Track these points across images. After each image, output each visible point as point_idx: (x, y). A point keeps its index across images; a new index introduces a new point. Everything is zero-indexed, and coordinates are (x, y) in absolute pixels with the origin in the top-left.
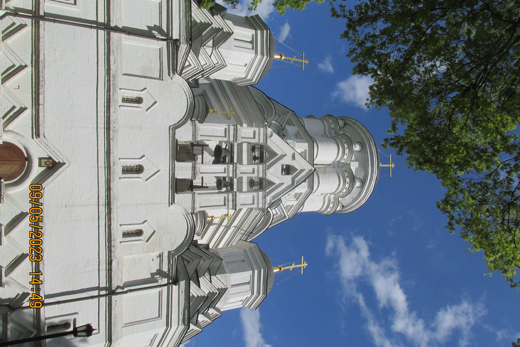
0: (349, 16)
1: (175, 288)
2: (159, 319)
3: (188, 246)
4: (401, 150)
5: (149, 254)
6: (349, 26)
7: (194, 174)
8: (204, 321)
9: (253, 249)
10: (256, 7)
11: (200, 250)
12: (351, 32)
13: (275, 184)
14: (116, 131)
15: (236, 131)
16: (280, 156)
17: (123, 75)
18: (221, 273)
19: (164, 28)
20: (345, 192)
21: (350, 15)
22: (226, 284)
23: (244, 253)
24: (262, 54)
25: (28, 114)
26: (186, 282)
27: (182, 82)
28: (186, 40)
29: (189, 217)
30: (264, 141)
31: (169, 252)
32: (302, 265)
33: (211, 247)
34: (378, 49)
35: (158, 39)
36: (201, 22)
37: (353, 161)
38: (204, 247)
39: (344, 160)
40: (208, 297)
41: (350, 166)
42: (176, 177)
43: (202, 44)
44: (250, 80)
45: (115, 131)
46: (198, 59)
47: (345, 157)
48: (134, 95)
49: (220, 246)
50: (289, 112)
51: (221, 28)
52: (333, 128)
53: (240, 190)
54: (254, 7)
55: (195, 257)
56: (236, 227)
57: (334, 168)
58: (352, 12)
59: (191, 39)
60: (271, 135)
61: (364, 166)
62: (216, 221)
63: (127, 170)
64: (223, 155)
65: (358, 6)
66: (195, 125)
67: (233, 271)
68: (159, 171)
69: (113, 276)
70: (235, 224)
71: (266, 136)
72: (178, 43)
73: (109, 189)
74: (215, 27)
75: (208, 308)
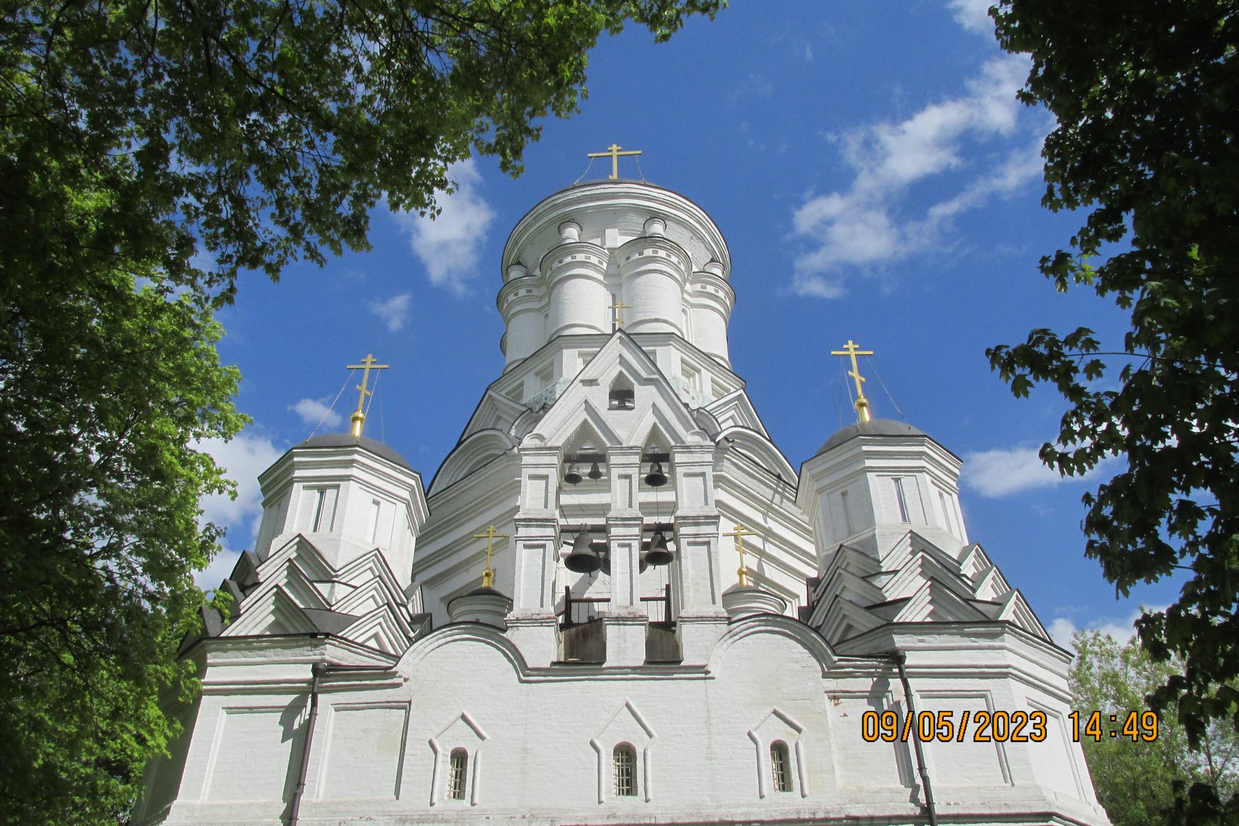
0: (232, 263)
1: (911, 659)
2: (990, 697)
3: (808, 631)
4: (529, 132)
5: (830, 724)
6: (254, 263)
7: (635, 619)
8: (992, 586)
9: (813, 472)
10: (228, 483)
11: (819, 601)
12: (267, 258)
13: (655, 425)
14: (534, 812)
15: (529, 522)
16: (589, 414)
17: (397, 798)
18: (875, 550)
19: (286, 700)
20: (678, 256)
21: (230, 261)
22: (900, 534)
23: (825, 494)
24: (350, 464)
26: (896, 634)
27: (415, 654)
28: (316, 646)
29: (738, 630)
30: (554, 455)
31: (825, 675)
32: (853, 353)
33: (813, 574)
34: (309, 192)
35: (313, 714)
36: (273, 612)
37: (604, 242)
38: (814, 591)
39: (602, 263)
40: (932, 579)
41: (614, 249)
42: (641, 663)
43: (325, 608)
44: (412, 493)
45: (533, 816)
46: (360, 618)
47: (594, 260)
48: (446, 770)
49: (811, 549)
50: (490, 396)
51: (287, 564)
52: (529, 291)
53: (672, 507)
54: (230, 488)
55: (837, 611)
56: (765, 515)
57: (620, 285)
58: (222, 256)
59: (313, 636)
60: (540, 437)
61: (614, 216)
62: (751, 562)
63: (628, 784)
64: (588, 551)
65: (207, 243)
66: (517, 619)
67: (870, 521)
68: (628, 705)
69: (887, 813)
70: (758, 518)
71: (541, 449)
72: (321, 667)
74: (286, 577)
75: (959, 576)
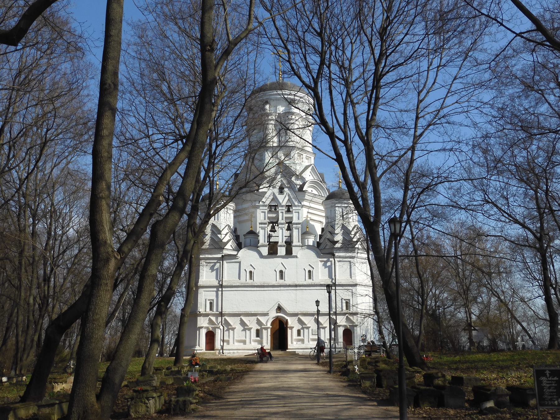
1: (336, 254)
25: (259, 318)
60: (263, 202)
63: (282, 277)
73: (290, 286)
